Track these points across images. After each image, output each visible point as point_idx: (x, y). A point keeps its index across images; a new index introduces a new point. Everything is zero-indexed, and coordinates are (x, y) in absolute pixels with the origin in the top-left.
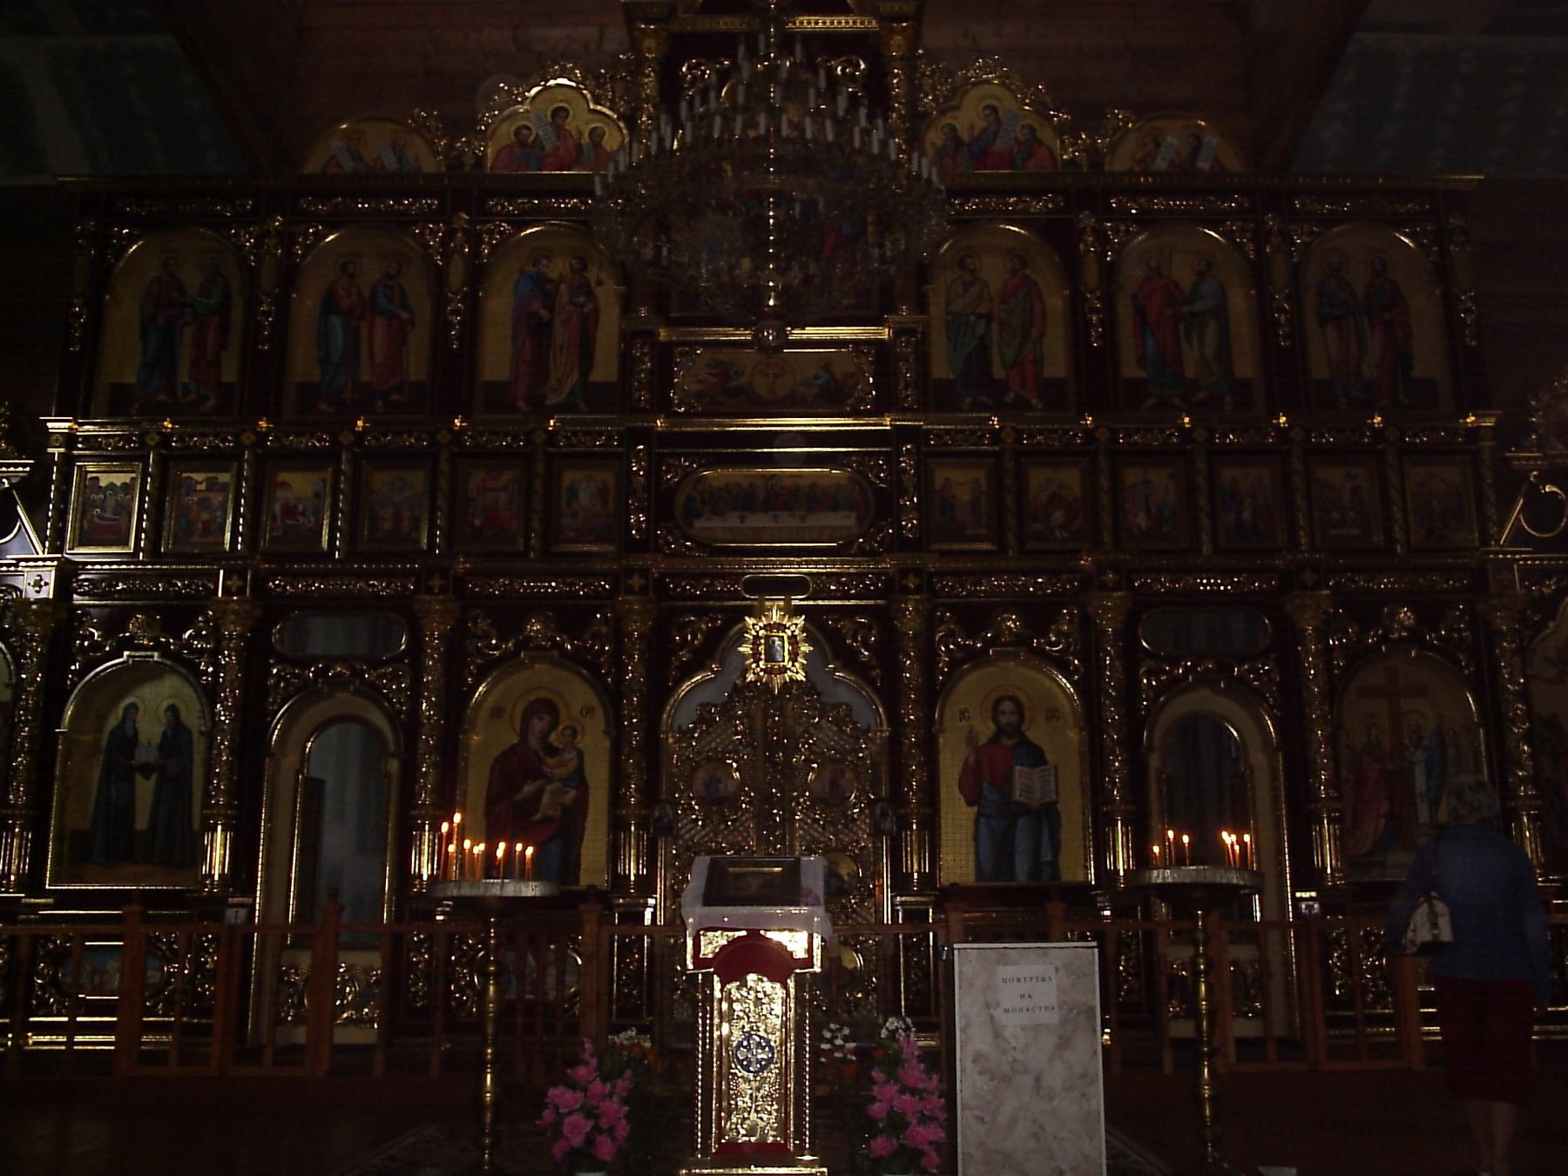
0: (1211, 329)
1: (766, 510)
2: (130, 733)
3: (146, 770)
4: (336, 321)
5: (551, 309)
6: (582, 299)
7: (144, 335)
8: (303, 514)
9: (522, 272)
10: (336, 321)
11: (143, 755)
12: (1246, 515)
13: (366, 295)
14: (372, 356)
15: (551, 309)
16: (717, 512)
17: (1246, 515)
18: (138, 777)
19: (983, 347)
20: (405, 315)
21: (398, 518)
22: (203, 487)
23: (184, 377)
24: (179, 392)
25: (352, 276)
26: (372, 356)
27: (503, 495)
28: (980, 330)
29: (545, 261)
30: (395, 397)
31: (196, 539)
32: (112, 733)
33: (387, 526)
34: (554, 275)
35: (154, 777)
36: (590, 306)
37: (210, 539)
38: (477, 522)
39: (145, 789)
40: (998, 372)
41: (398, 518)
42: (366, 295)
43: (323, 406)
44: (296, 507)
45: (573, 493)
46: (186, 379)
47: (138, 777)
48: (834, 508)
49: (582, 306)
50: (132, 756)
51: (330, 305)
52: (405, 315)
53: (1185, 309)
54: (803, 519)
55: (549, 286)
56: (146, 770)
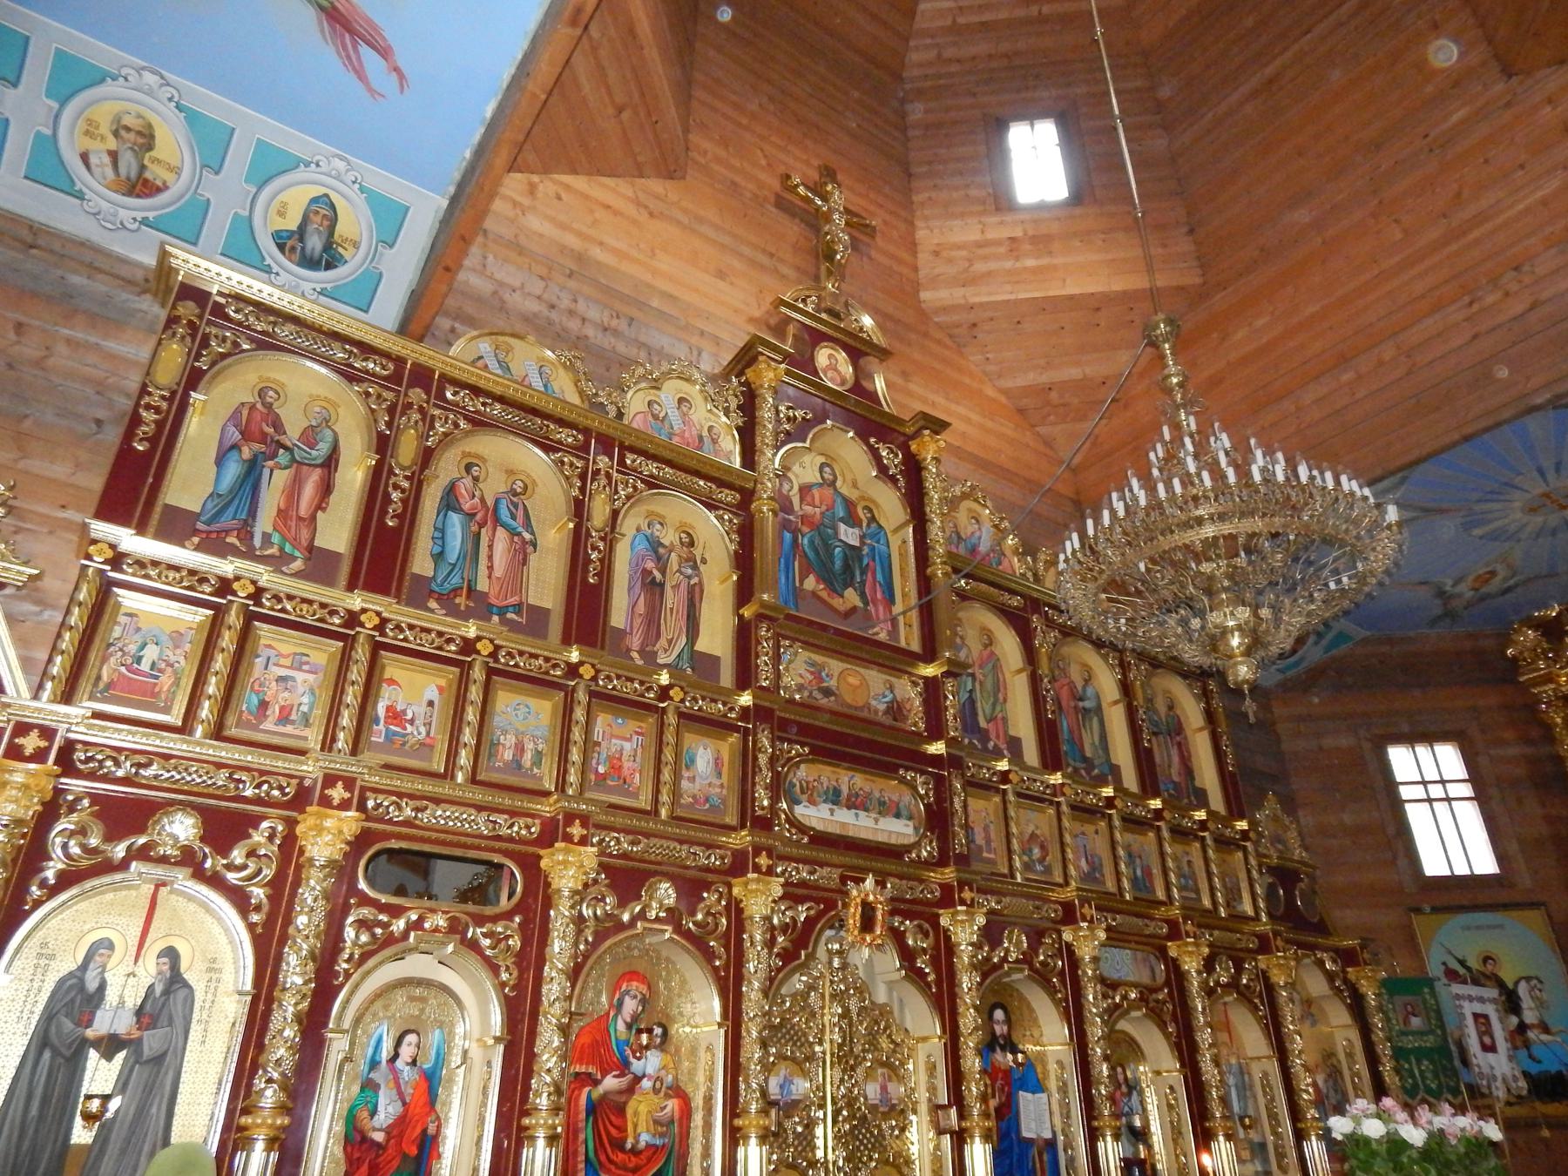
0: (1095, 720)
1: (849, 808)
2: (92, 985)
3: (110, 1045)
4: (455, 519)
5: (663, 573)
6: (690, 571)
7: (220, 461)
8: (412, 722)
9: (638, 530)
10: (455, 519)
11: (114, 1017)
12: (1139, 872)
13: (490, 502)
14: (490, 568)
15: (663, 573)
16: (812, 802)
17: (1139, 872)
18: (93, 1055)
19: (972, 701)
20: (527, 536)
21: (520, 749)
22: (288, 662)
23: (265, 522)
24: (257, 542)
25: (476, 479)
26: (490, 568)
27: (627, 746)
28: (969, 687)
29: (658, 526)
30: (510, 616)
31: (268, 725)
32: (61, 982)
33: (508, 755)
34: (666, 542)
35: (120, 1056)
36: (695, 580)
37: (289, 729)
38: (601, 770)
39: (100, 1075)
40: (983, 724)
41: (520, 749)
42: (490, 502)
43: (433, 604)
44: (404, 712)
45: (693, 761)
46: (269, 530)
47: (93, 1055)
48: (898, 816)
49: (689, 577)
50: (89, 1024)
51: (450, 501)
52: (527, 536)
53: (1081, 704)
54: (876, 821)
55: (661, 550)
56: (110, 1045)
